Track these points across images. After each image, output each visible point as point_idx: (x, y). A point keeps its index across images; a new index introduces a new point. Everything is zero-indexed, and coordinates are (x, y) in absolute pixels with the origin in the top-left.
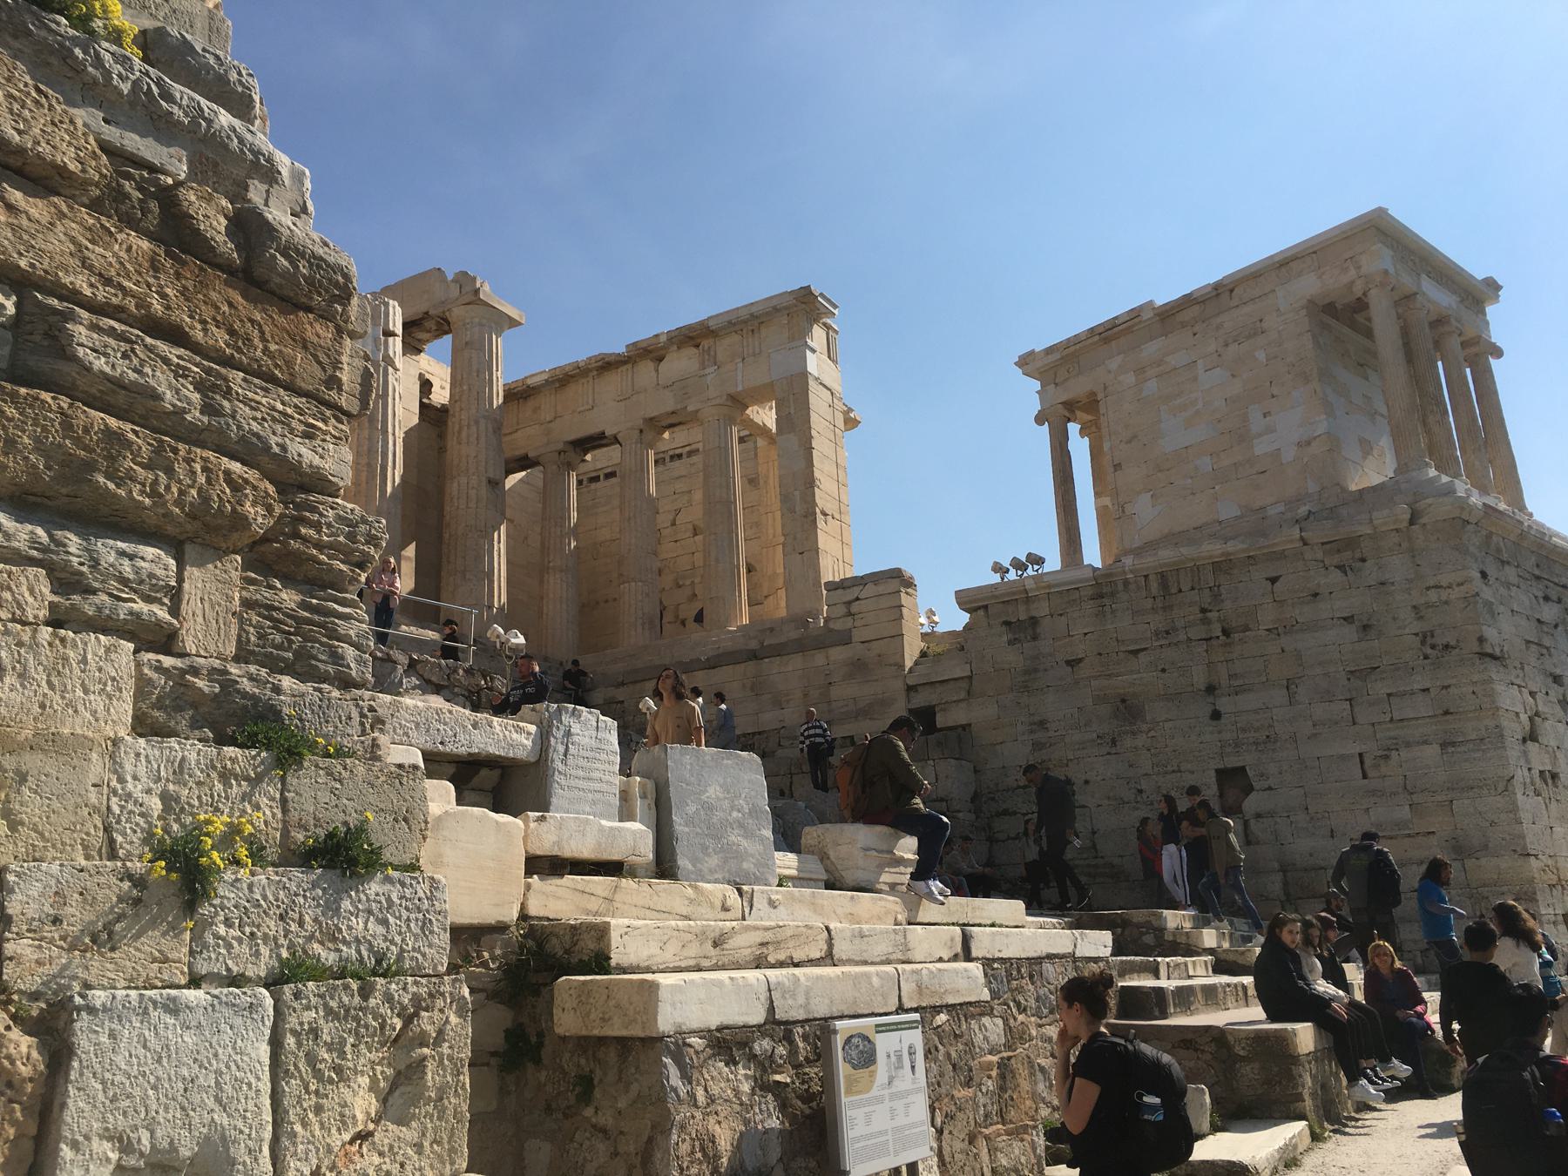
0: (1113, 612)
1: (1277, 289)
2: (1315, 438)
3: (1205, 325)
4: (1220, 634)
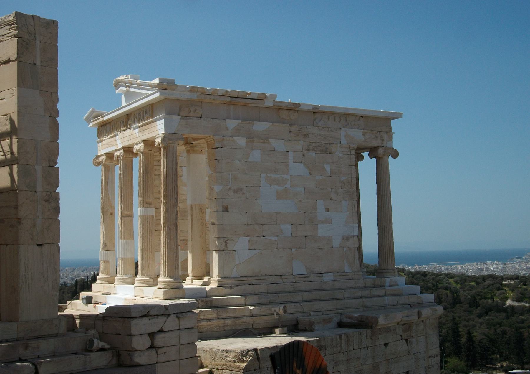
1: (343, 129)
2: (351, 237)
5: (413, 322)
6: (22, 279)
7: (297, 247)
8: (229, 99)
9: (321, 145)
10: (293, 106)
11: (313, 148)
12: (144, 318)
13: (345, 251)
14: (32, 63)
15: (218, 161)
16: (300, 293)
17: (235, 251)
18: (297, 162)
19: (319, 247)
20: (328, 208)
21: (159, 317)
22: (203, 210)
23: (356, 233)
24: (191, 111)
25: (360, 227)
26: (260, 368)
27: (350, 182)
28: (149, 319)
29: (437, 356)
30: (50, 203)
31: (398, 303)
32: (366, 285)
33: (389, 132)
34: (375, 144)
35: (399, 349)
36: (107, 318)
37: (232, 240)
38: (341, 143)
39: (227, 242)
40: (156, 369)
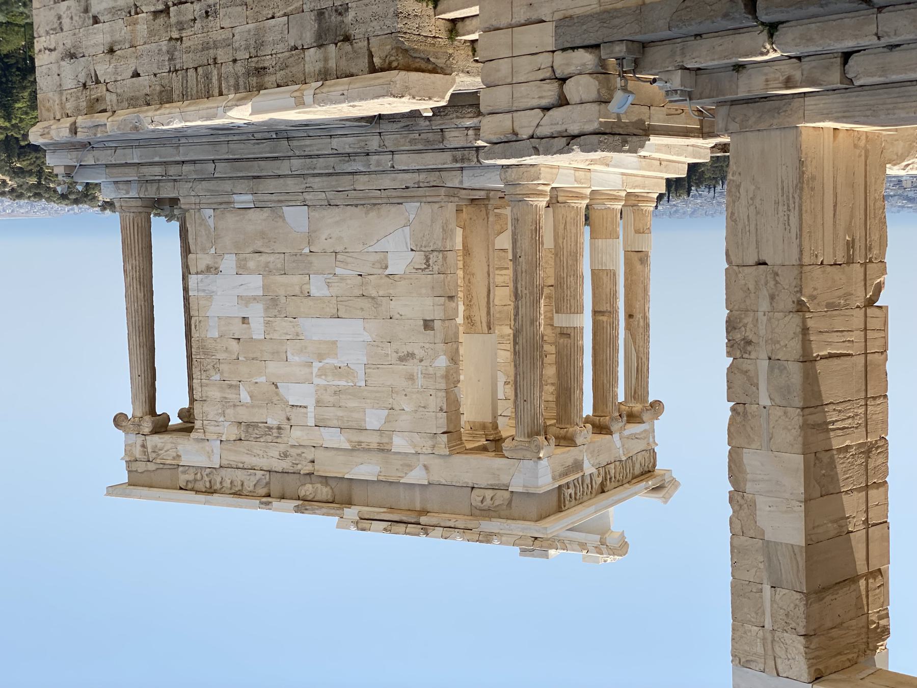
0: (247, 48)
2: (202, 272)
3: (299, 467)
4: (171, 9)
5: (86, 114)
6: (794, 203)
7: (301, 255)
8: (423, 520)
9: (257, 438)
10: (307, 507)
11: (270, 433)
12: (576, 132)
13: (214, 247)
14: (778, 589)
15: (441, 410)
16: (295, 173)
17: (412, 250)
18: (301, 406)
19: (261, 255)
20: (244, 325)
21: (549, 134)
22: (469, 323)
23: (193, 280)
24: (492, 499)
25: (186, 290)
26: (368, 39)
27: (204, 371)
28: (566, 130)
29: (40, 51)
30: (744, 339)
31: (114, 151)
32: (174, 185)
33: (131, 462)
34: (156, 440)
35: (112, 65)
36: (644, 133)
37: (417, 269)
38: (221, 441)
39: (426, 266)
40: (556, 40)
